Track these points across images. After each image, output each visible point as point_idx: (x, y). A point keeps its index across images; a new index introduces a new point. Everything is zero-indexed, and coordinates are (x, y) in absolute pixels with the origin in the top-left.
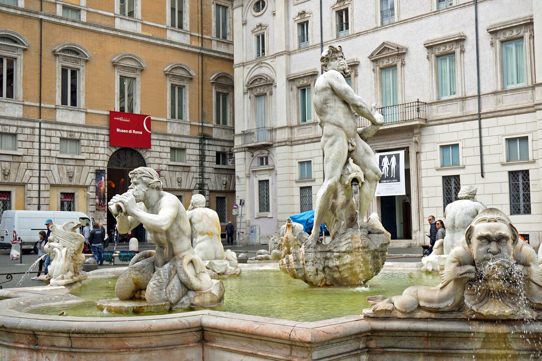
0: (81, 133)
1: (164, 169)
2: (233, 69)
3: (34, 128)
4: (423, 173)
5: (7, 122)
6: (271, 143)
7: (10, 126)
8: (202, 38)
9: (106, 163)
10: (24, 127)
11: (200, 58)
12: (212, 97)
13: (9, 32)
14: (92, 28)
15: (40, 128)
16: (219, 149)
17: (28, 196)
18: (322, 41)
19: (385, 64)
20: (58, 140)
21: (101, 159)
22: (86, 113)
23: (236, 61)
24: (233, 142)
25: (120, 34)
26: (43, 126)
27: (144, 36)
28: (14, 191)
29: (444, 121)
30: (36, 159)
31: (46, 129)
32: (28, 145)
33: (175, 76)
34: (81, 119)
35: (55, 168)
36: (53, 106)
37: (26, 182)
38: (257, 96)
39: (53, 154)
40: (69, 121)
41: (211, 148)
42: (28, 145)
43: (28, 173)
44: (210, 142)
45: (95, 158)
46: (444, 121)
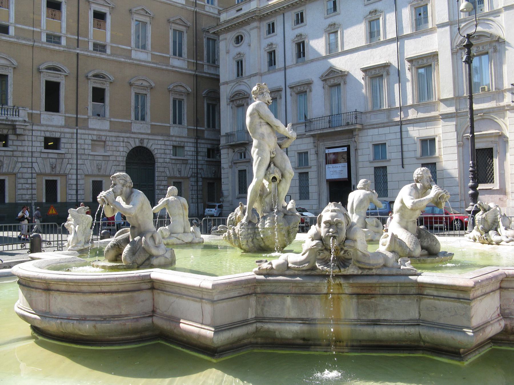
0: (106, 136)
1: (168, 162)
2: (219, 87)
3: (73, 133)
4: (360, 165)
5: (54, 129)
6: (247, 142)
7: (56, 132)
8: (196, 63)
9: (125, 158)
11: (195, 78)
12: (204, 107)
14: (114, 58)
15: (77, 133)
16: (209, 146)
17: (69, 183)
18: (285, 66)
19: (332, 83)
20: (90, 142)
21: (121, 155)
22: (110, 121)
23: (222, 80)
24: (219, 140)
25: (135, 62)
27: (153, 63)
28: (58, 179)
29: (375, 126)
30: (75, 156)
31: (81, 134)
32: (68, 146)
33: (176, 92)
34: (106, 125)
35: (87, 162)
36: (86, 117)
37: (68, 173)
38: (238, 106)
39: (87, 152)
40: (98, 127)
41: (202, 146)
42: (68, 146)
43: (69, 166)
44: (203, 141)
45: (117, 155)
46: (375, 126)
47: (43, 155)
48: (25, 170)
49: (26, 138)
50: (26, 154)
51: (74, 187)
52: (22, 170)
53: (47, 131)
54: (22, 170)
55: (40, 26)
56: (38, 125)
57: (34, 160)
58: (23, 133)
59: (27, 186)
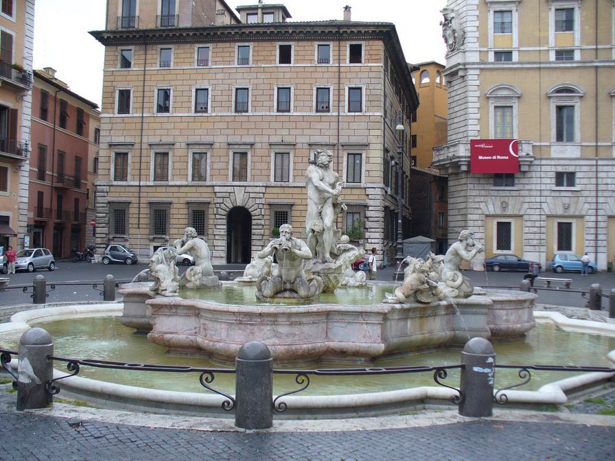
3: (593, 165)
10: (582, 165)
13: (566, 84)
26: (600, 162)
28: (573, 221)
32: (586, 181)
42: (586, 181)
43: (587, 206)
47: (553, 194)
48: (532, 212)
49: (534, 174)
50: (534, 193)
51: (593, 231)
52: (529, 211)
53: (559, 165)
54: (529, 211)
55: (548, 43)
56: (547, 159)
57: (543, 199)
58: (527, 170)
59: (535, 229)
